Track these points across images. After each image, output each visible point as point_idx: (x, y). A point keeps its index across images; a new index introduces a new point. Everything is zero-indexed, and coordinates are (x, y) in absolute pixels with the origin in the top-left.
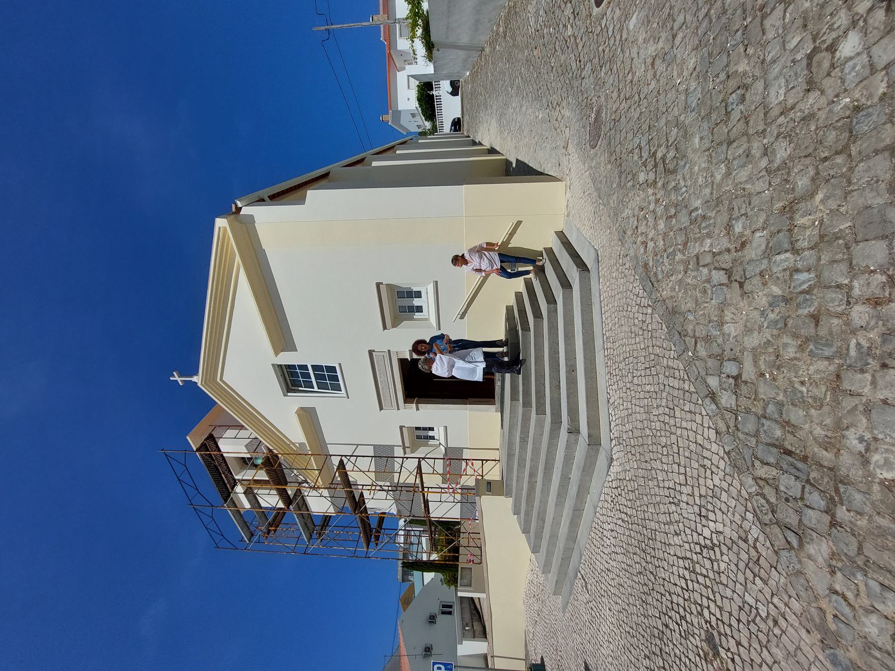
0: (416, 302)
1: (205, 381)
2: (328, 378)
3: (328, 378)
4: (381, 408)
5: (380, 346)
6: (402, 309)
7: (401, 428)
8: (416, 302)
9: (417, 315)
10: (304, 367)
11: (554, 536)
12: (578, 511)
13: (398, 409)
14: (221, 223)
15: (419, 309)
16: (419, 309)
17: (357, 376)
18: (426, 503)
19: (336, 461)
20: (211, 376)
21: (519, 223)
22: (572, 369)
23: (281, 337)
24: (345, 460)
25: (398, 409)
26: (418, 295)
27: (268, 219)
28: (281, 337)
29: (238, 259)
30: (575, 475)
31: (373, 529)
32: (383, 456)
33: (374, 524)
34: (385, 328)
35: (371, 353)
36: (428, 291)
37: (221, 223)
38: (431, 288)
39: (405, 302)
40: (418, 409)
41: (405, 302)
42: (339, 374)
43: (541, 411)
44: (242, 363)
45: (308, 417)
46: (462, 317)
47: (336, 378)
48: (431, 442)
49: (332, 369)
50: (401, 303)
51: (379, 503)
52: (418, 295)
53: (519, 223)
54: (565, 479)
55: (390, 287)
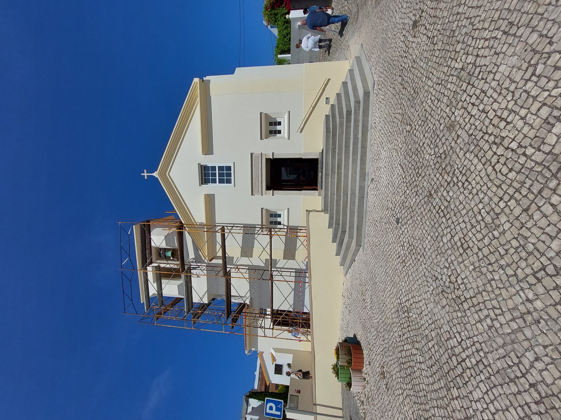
0: (278, 128)
1: (160, 174)
2: (225, 175)
3: (225, 175)
4: (252, 194)
5: (257, 152)
6: (271, 132)
8: (278, 128)
9: (278, 135)
10: (214, 168)
11: (353, 194)
12: (364, 147)
13: (262, 195)
14: (196, 80)
15: (279, 132)
16: (279, 132)
17: (242, 174)
18: (272, 276)
20: (163, 174)
21: (329, 80)
23: (208, 149)
25: (262, 195)
26: (280, 124)
28: (208, 149)
29: (199, 99)
30: (360, 136)
31: (234, 312)
32: (249, 231)
33: (234, 308)
34: (261, 139)
35: (252, 154)
37: (196, 80)
39: (272, 128)
40: (273, 195)
41: (272, 128)
44: (180, 172)
45: (210, 200)
46: (301, 132)
47: (229, 175)
48: (279, 226)
49: (229, 168)
50: (271, 127)
51: (241, 289)
52: (280, 124)
53: (329, 80)
55: (266, 115)
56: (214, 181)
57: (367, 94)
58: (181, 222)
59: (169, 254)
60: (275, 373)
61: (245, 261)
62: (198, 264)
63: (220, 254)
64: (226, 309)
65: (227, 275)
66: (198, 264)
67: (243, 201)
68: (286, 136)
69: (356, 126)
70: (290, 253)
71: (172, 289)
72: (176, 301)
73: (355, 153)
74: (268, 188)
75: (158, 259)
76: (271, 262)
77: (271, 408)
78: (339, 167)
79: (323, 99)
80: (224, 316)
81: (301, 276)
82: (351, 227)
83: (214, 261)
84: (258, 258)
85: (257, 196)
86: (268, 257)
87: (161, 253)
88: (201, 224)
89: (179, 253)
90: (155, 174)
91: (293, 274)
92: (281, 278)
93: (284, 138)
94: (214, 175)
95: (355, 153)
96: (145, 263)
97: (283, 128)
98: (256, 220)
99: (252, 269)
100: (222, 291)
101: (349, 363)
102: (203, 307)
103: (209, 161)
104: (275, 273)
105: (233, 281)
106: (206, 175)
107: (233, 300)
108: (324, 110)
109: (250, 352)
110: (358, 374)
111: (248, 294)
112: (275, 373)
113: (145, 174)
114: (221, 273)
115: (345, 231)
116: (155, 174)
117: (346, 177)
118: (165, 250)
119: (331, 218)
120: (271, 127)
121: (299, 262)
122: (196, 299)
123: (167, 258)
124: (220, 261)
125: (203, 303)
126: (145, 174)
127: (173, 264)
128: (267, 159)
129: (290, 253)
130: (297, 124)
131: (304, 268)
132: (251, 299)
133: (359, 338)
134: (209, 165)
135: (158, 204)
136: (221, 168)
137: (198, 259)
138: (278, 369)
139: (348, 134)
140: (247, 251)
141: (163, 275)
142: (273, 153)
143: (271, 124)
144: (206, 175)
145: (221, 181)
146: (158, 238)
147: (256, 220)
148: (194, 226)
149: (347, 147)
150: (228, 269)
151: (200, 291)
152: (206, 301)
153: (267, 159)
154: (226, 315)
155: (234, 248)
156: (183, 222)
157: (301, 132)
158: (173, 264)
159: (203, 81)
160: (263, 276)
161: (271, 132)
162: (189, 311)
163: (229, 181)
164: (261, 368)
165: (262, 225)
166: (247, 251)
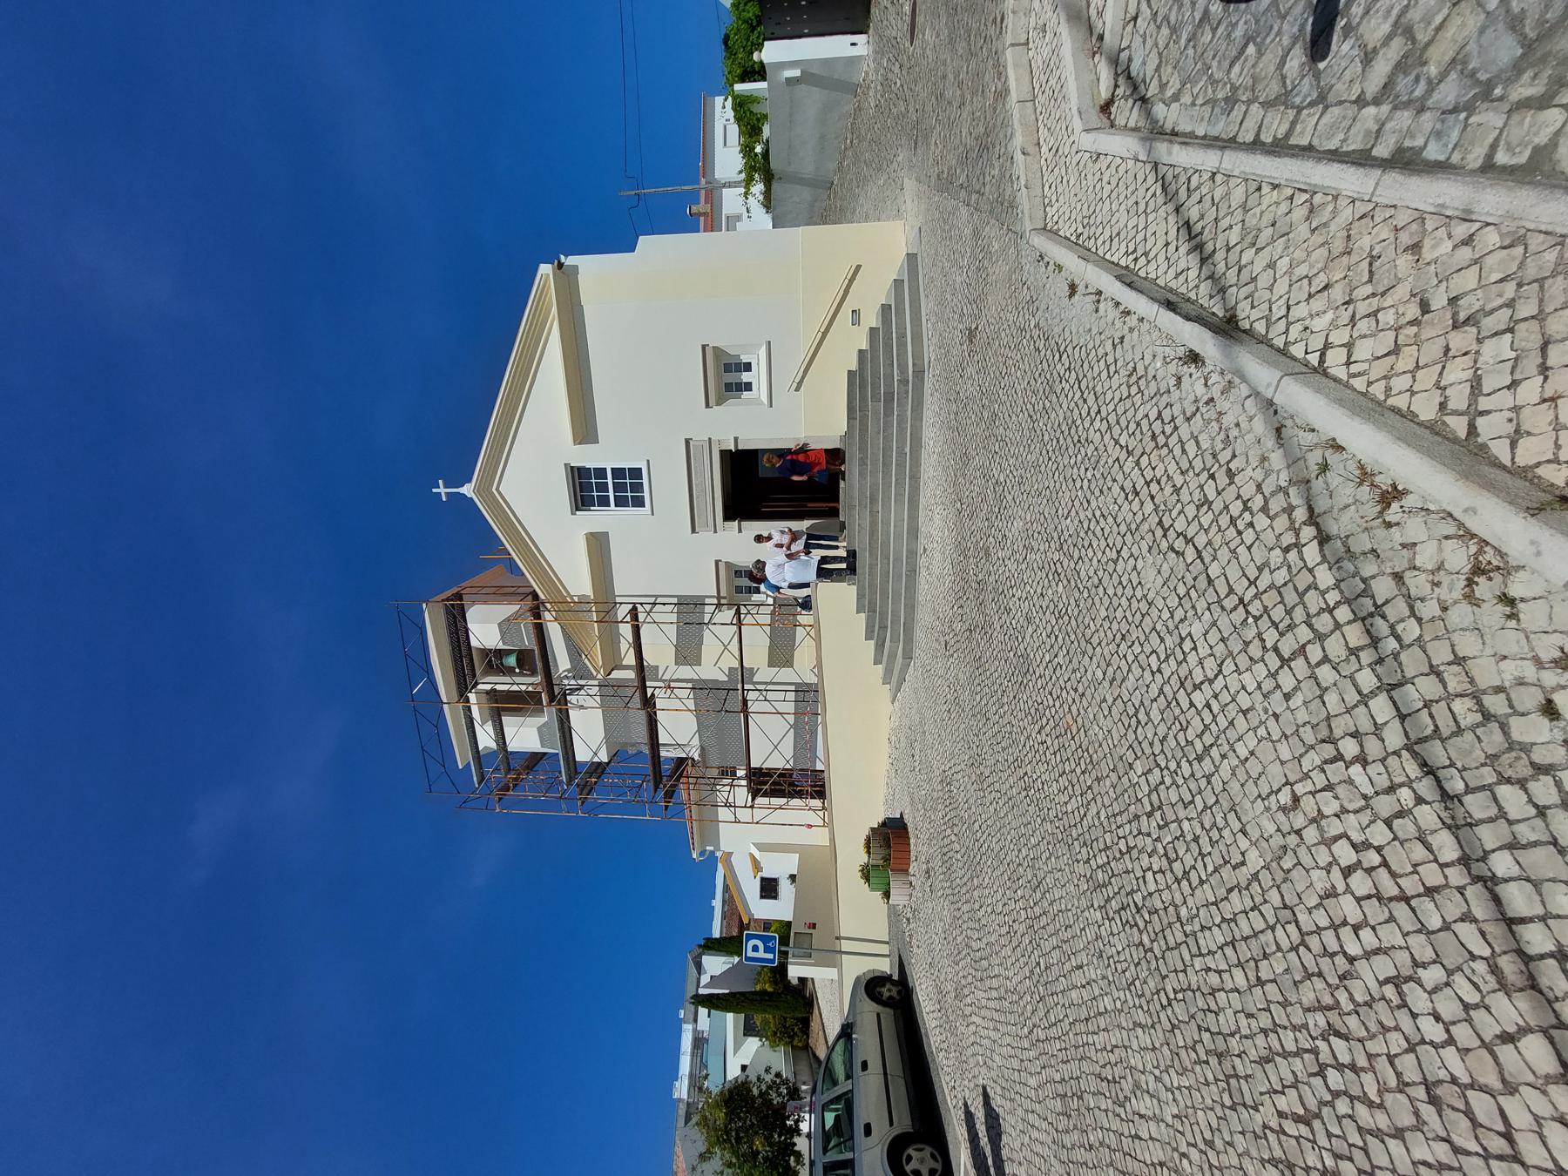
0: (745, 377)
1: (478, 491)
2: (628, 487)
3: (628, 487)
4: (693, 531)
5: (699, 436)
6: (729, 387)
7: (717, 562)
8: (745, 377)
10: (601, 472)
12: (915, 478)
14: (545, 269)
15: (748, 387)
16: (748, 387)
17: (668, 485)
18: (745, 702)
19: (623, 611)
20: (485, 489)
21: (859, 267)
22: (902, 336)
24: (640, 608)
26: (748, 367)
27: (591, 268)
29: (554, 309)
31: (666, 776)
32: (690, 610)
34: (707, 405)
35: (687, 442)
36: (759, 359)
37: (545, 269)
38: (763, 352)
39: (731, 378)
41: (731, 378)
42: (645, 481)
43: (876, 398)
45: (599, 545)
46: (797, 390)
49: (636, 473)
50: (728, 377)
51: (679, 729)
52: (748, 367)
53: (859, 267)
54: (901, 453)
56: (604, 502)
57: (919, 373)
58: (535, 596)
59: (511, 661)
60: (762, 897)
61: (686, 672)
62: (582, 682)
63: (630, 659)
64: (650, 772)
65: (648, 703)
66: (582, 682)
67: (674, 547)
68: (765, 399)
69: (901, 429)
70: (781, 654)
71: (525, 735)
72: (534, 759)
73: (900, 484)
74: (729, 516)
75: (486, 673)
76: (743, 674)
77: (755, 949)
78: (873, 500)
79: (846, 312)
80: (648, 786)
81: (808, 698)
82: (895, 622)
83: (616, 674)
84: (715, 664)
85: (705, 536)
86: (736, 664)
87: (494, 661)
88: (583, 601)
89: (536, 659)
90: (467, 490)
91: (791, 696)
92: (767, 707)
93: (758, 401)
94: (604, 487)
95: (900, 484)
96: (464, 683)
97: (758, 377)
98: (705, 585)
99: (699, 687)
100: (640, 735)
101: (887, 859)
102: (598, 769)
103: (589, 457)
104: (751, 696)
105: (660, 716)
106: (586, 488)
107: (663, 753)
108: (848, 344)
109: (702, 853)
110: (902, 877)
111: (696, 741)
112: (762, 897)
113: (442, 490)
114: (637, 701)
115: (888, 628)
116: (467, 490)
117: (887, 523)
118: (500, 654)
119: (860, 597)
120: (728, 377)
121: (803, 669)
122: (582, 755)
123: (509, 671)
124: (631, 674)
125: (600, 764)
126: (442, 490)
127: (523, 683)
128: (722, 452)
129: (781, 654)
130: (788, 372)
131: (814, 680)
132: (702, 749)
133: (908, 819)
134: (591, 464)
135: (476, 551)
136: (618, 473)
137: (579, 671)
138: (769, 888)
139: (888, 439)
140: (688, 652)
141: (503, 705)
142: (736, 439)
143: (728, 368)
144: (586, 488)
145: (620, 502)
146: (485, 628)
147: (705, 585)
148: (570, 609)
149: (887, 465)
150: (649, 692)
151: (591, 737)
152: (603, 757)
153: (722, 452)
154: (651, 785)
155: (659, 648)
156: (542, 597)
157: (797, 390)
158: (523, 683)
159: (560, 265)
160: (725, 701)
161: (729, 387)
162: (569, 783)
163: (639, 502)
164: (726, 888)
165: (719, 597)
166: (688, 652)
